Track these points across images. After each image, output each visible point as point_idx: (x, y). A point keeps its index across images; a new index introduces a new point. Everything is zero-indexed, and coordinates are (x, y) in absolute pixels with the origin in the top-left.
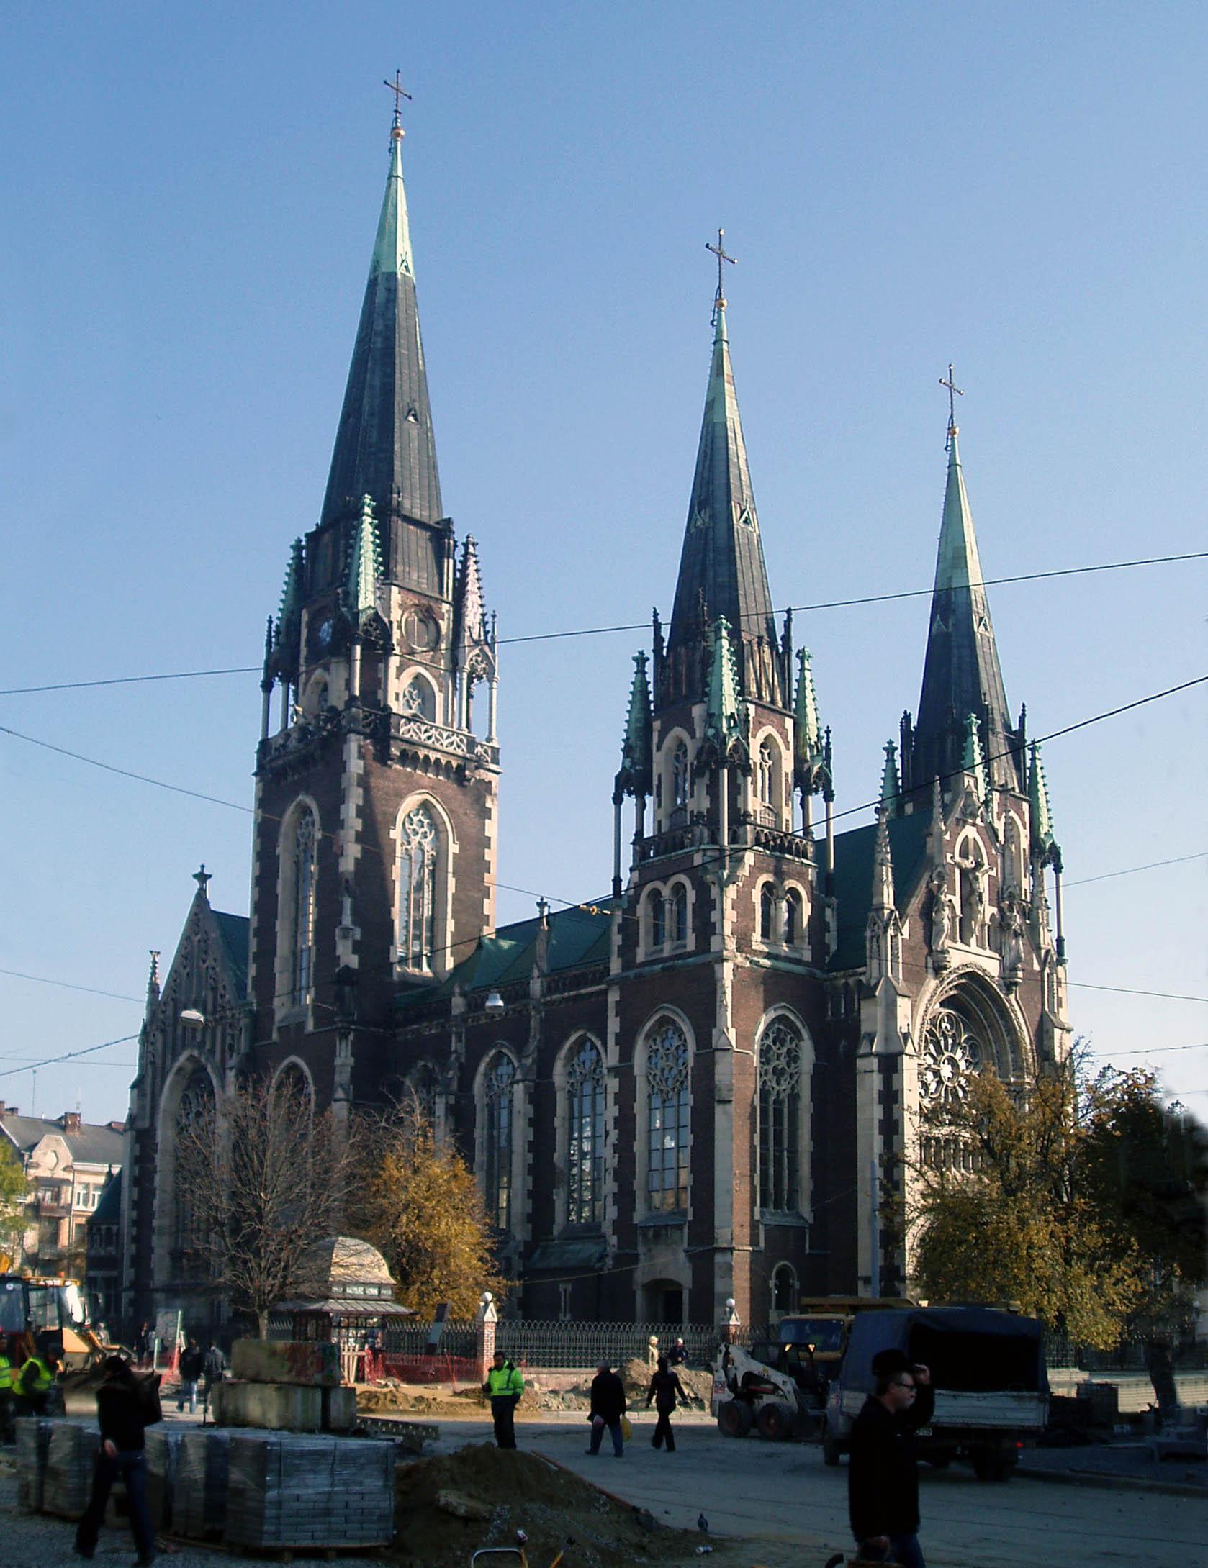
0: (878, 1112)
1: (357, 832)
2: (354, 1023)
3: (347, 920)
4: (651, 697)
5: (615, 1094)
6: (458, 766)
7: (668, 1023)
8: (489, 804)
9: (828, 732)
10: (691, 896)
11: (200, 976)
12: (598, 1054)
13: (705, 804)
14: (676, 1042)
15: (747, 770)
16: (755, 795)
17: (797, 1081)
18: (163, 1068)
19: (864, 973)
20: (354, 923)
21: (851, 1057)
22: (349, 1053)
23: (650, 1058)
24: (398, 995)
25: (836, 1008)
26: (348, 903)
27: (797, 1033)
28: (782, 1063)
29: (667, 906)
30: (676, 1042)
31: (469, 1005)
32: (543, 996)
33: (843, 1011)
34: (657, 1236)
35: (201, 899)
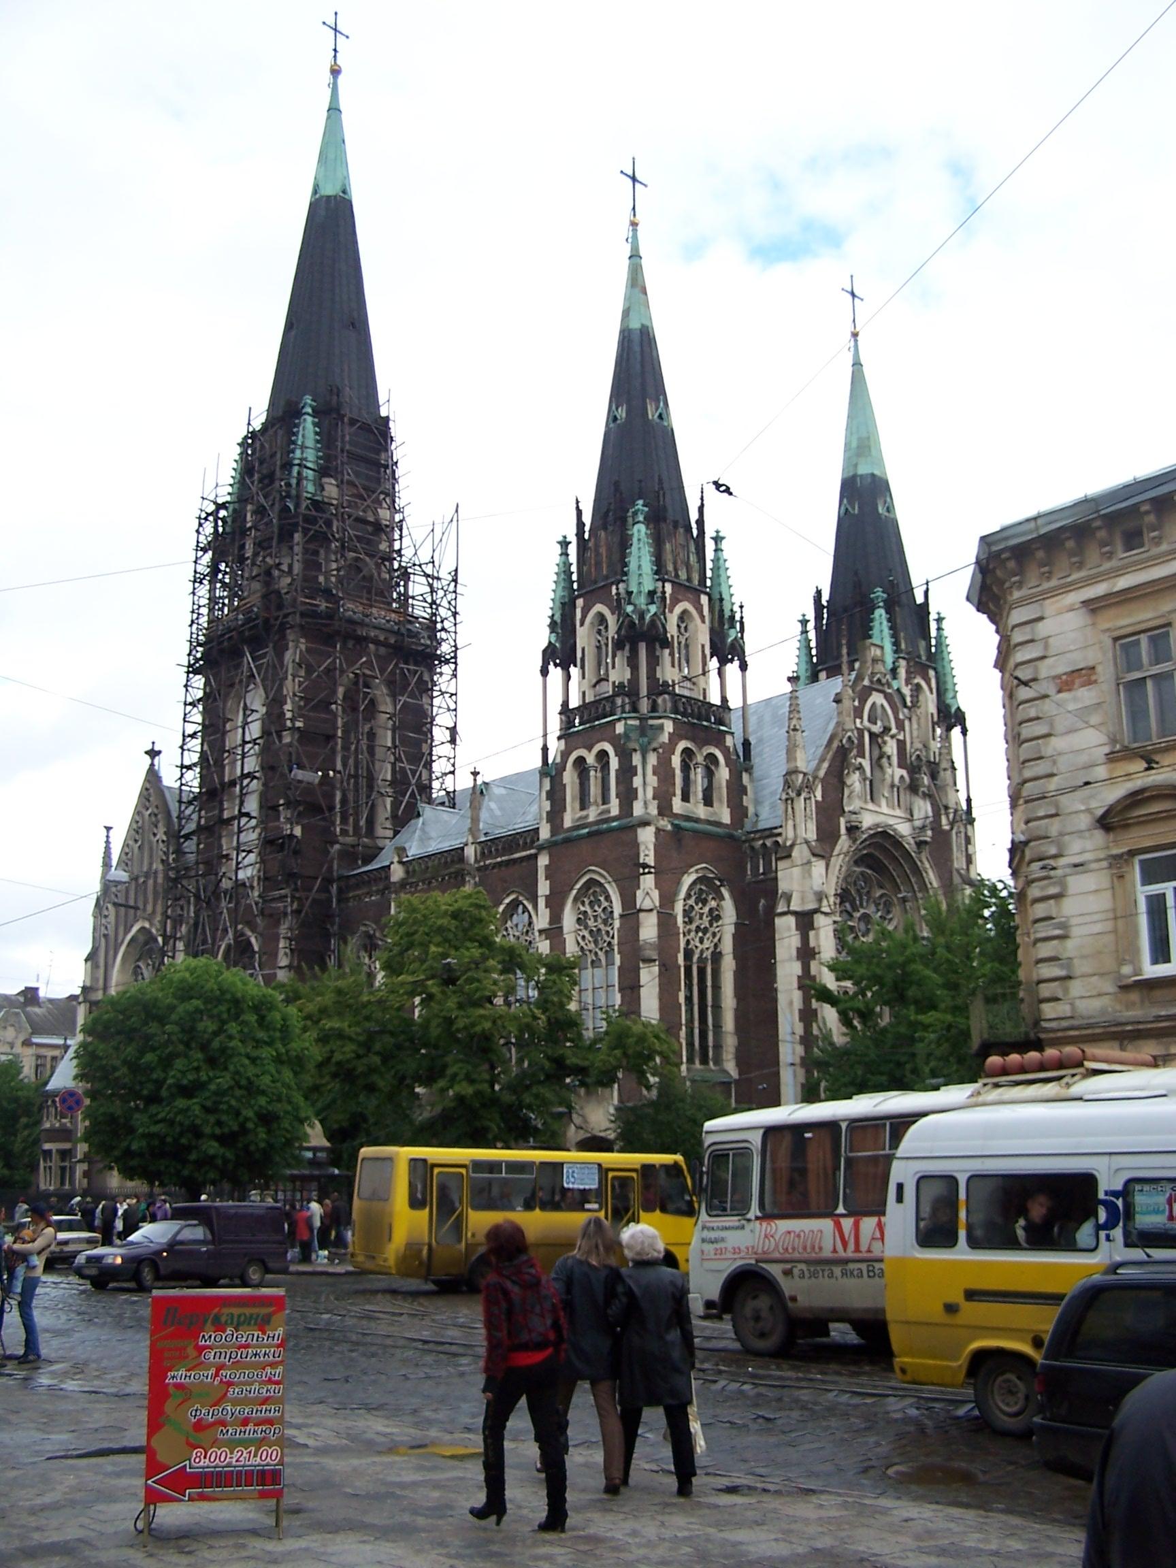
0: (796, 968)
4: (574, 577)
9: (741, 607)
10: (614, 763)
11: (151, 849)
12: (530, 916)
13: (628, 675)
15: (666, 643)
16: (673, 666)
17: (719, 940)
18: (116, 940)
19: (780, 834)
21: (771, 914)
23: (579, 919)
25: (755, 868)
28: (706, 920)
29: (592, 773)
30: (605, 904)
31: (407, 872)
32: (476, 861)
35: (153, 776)
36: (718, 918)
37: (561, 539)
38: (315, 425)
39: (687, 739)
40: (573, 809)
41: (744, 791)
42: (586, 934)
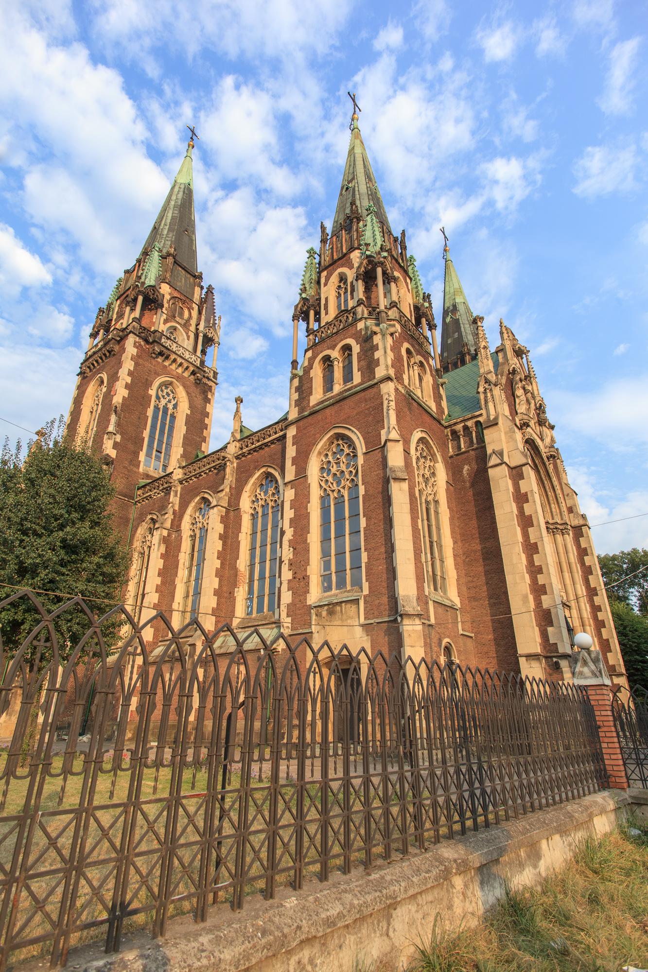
3: (111, 428)
5: (291, 501)
6: (193, 371)
8: (209, 396)
10: (356, 349)
12: (277, 482)
19: (481, 415)
24: (140, 480)
26: (113, 418)
27: (433, 456)
28: (427, 474)
29: (336, 363)
30: (347, 451)
34: (331, 613)
36: (434, 474)
41: (441, 397)
42: (330, 479)
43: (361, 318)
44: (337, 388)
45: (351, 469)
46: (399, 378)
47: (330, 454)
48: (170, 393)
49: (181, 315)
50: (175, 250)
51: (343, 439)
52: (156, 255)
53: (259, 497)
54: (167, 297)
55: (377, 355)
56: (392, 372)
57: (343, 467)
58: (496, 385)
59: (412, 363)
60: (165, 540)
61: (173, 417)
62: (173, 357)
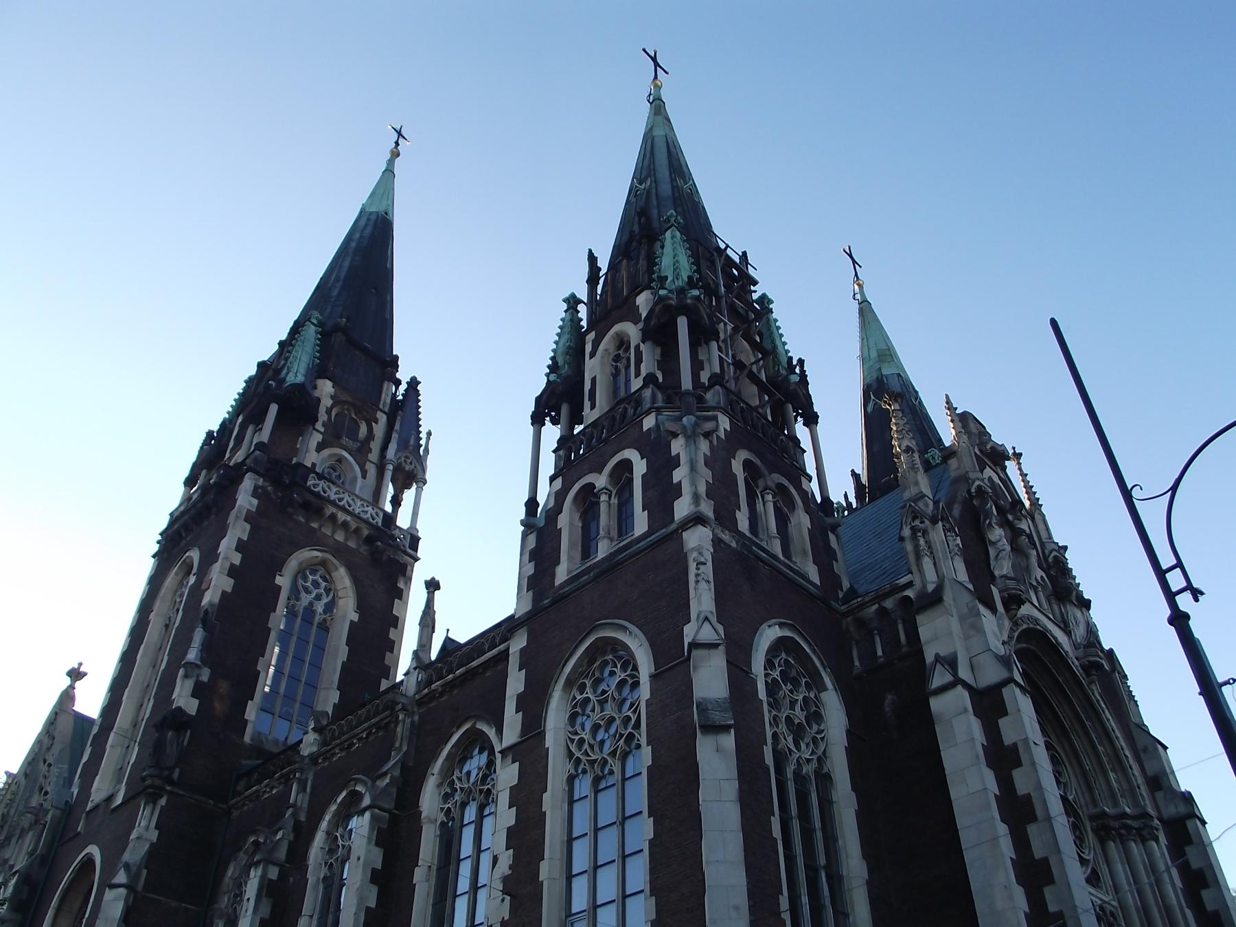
1: (232, 565)
2: (170, 782)
3: (192, 655)
7: (604, 653)
8: (401, 585)
10: (640, 467)
14: (620, 675)
19: (910, 585)
20: (202, 660)
22: (153, 824)
23: (573, 718)
25: (868, 654)
26: (199, 635)
28: (799, 715)
29: (604, 498)
31: (324, 743)
33: (880, 653)
37: (567, 295)
38: (316, 333)
39: (750, 450)
40: (570, 558)
41: (832, 555)
42: (586, 735)
43: (650, 409)
44: (603, 549)
45: (629, 713)
46: (725, 518)
47: (588, 685)
48: (320, 580)
49: (353, 434)
50: (348, 319)
51: (614, 651)
52: (311, 332)
53: (458, 785)
54: (327, 402)
55: (679, 475)
56: (707, 509)
57: (609, 710)
58: (934, 521)
59: (761, 489)
60: (267, 888)
61: (324, 628)
62: (330, 510)
